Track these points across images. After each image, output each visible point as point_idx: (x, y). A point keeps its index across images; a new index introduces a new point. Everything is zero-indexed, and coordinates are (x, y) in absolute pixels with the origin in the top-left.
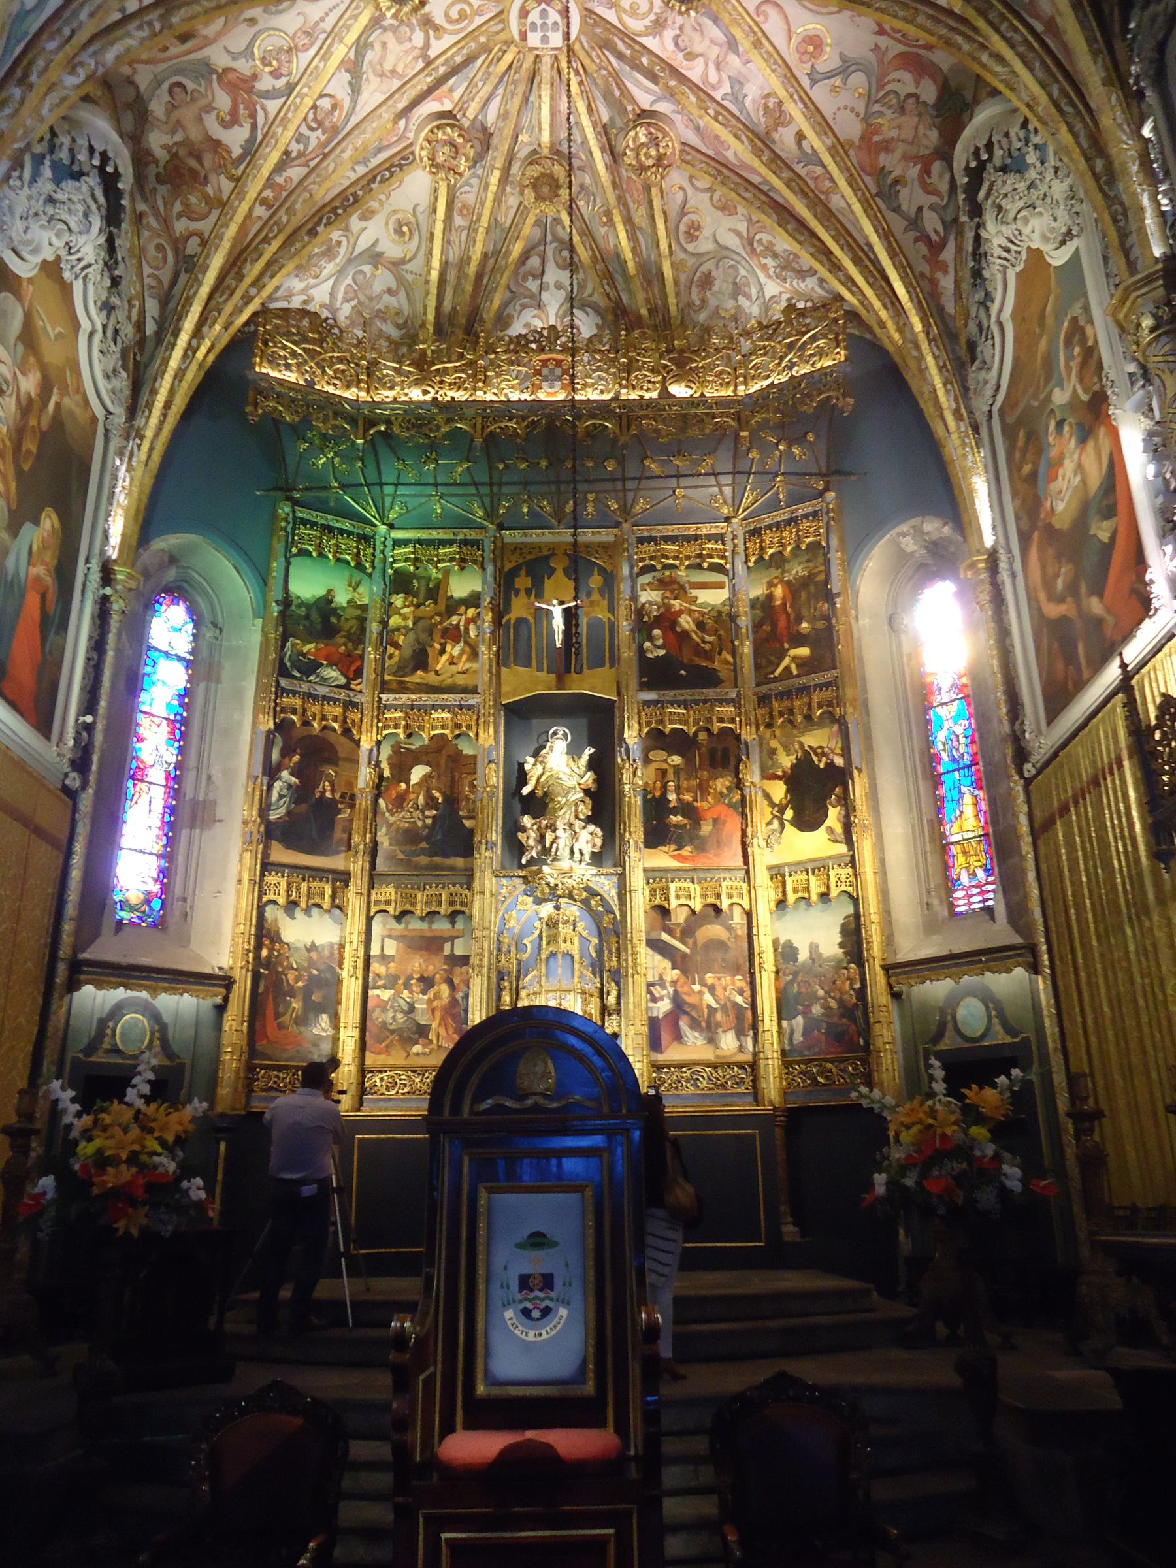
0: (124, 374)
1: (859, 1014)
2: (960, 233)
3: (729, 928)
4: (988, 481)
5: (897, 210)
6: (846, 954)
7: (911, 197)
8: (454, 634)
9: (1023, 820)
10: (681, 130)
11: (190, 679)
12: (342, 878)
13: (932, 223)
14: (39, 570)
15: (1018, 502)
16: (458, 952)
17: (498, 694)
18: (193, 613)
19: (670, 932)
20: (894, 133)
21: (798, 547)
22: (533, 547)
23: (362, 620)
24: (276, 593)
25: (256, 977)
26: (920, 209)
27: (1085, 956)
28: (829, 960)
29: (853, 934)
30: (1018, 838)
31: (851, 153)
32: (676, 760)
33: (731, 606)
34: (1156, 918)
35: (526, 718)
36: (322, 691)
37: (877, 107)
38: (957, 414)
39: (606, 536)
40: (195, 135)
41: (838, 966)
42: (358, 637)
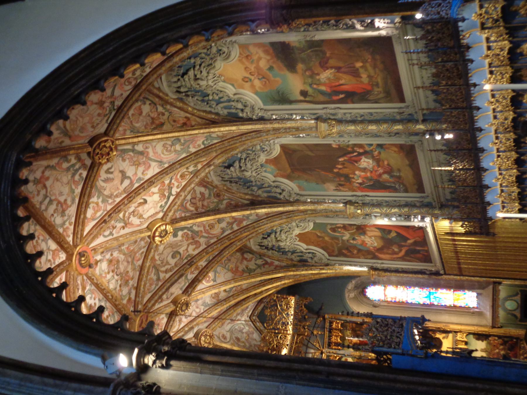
1: (506, 339)
2: (264, 255)
4: (346, 265)
5: (255, 270)
6: (486, 340)
7: (252, 265)
9: (455, 277)
10: (203, 327)
13: (259, 262)
15: (363, 257)
20: (234, 264)
21: (341, 331)
26: (256, 264)
27: (501, 267)
28: (487, 346)
29: (479, 336)
30: (461, 280)
31: (236, 277)
33: (355, 358)
34: (498, 245)
37: (227, 266)
38: (321, 269)
41: (489, 343)
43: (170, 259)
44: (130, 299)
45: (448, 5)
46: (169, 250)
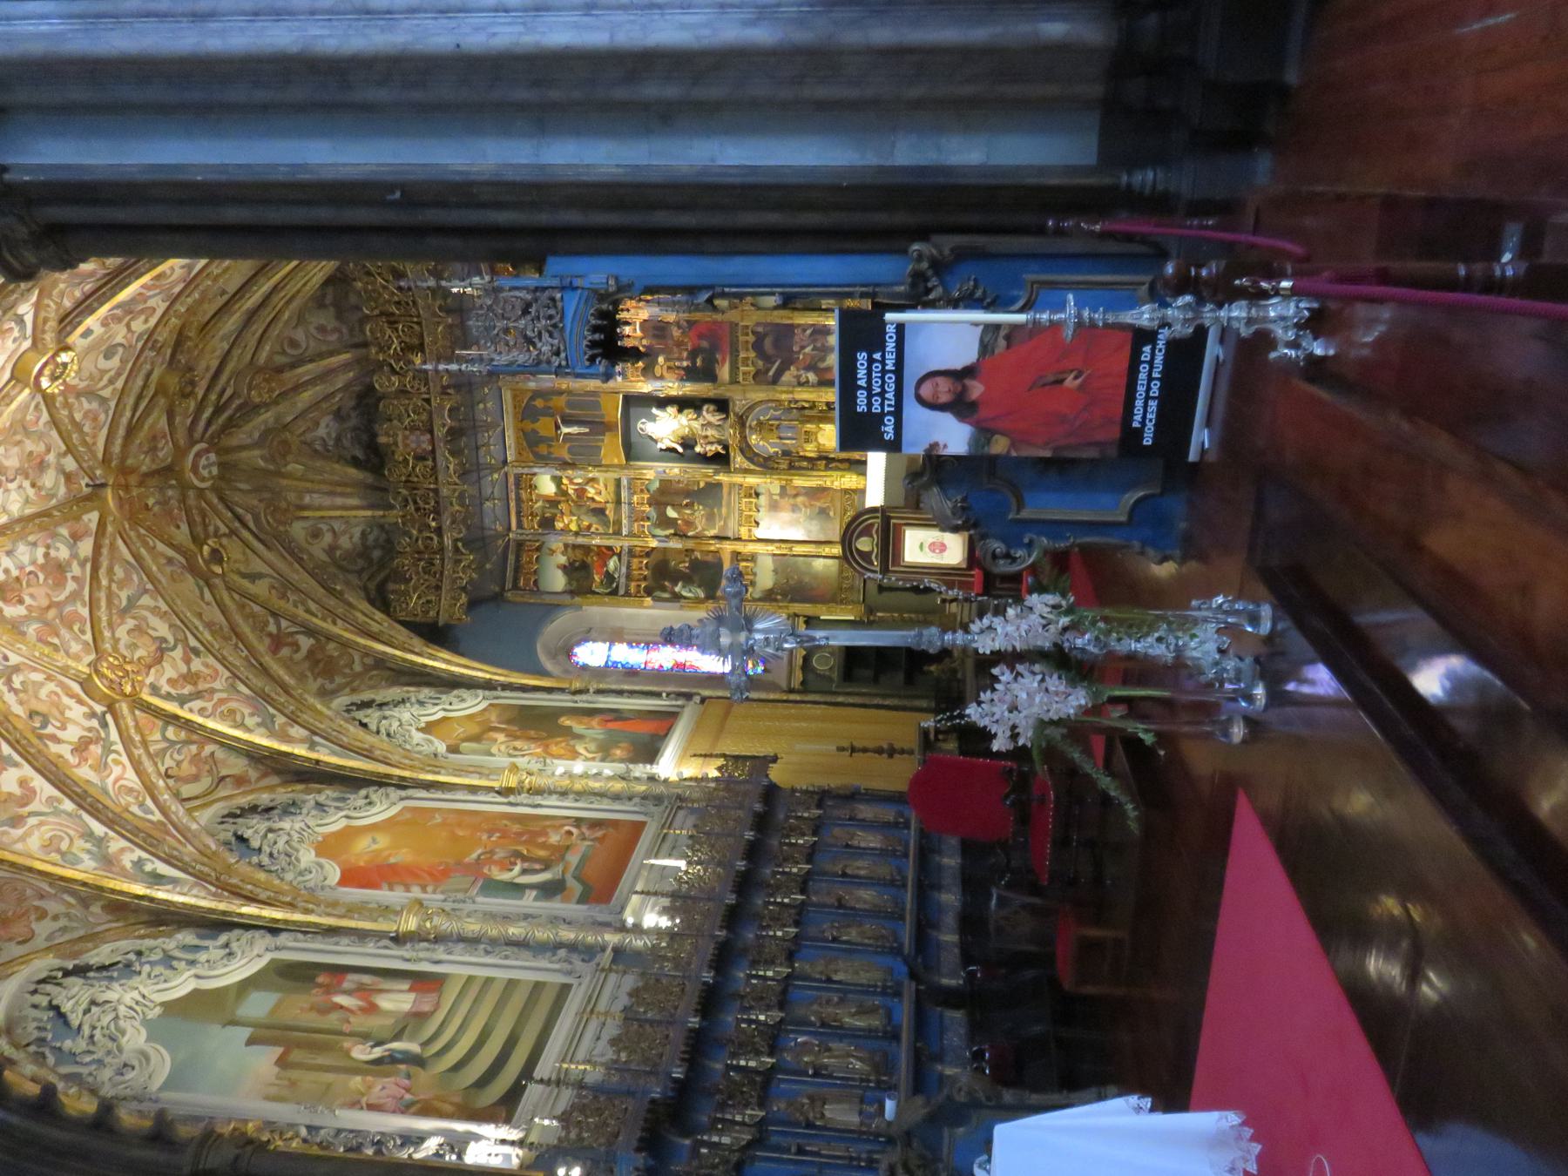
0: (455, 692)
3: (765, 335)
8: (581, 492)
11: (621, 641)
12: (736, 555)
14: (595, 722)
16: (778, 491)
17: (620, 467)
18: (578, 644)
19: (768, 370)
22: (518, 443)
23: (575, 547)
24: (567, 599)
25: (792, 601)
32: (661, 359)
35: (633, 450)
36: (624, 570)
39: (507, 396)
40: (307, 664)
42: (587, 549)
43: (103, 364)
44: (69, 477)
45: (552, 312)
46: (91, 357)
